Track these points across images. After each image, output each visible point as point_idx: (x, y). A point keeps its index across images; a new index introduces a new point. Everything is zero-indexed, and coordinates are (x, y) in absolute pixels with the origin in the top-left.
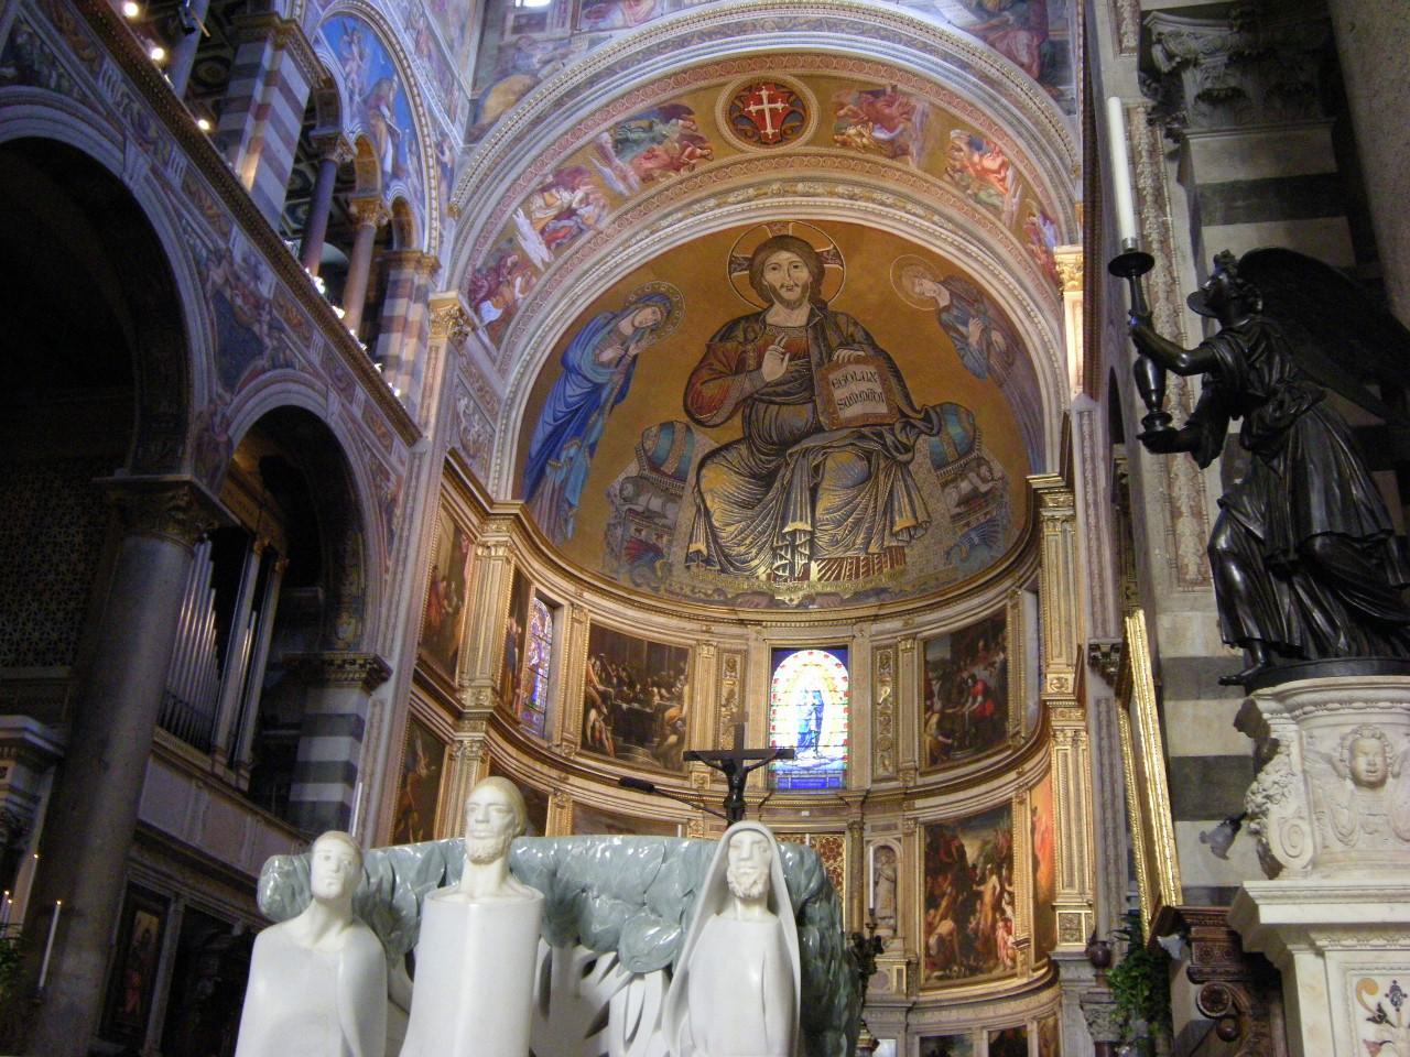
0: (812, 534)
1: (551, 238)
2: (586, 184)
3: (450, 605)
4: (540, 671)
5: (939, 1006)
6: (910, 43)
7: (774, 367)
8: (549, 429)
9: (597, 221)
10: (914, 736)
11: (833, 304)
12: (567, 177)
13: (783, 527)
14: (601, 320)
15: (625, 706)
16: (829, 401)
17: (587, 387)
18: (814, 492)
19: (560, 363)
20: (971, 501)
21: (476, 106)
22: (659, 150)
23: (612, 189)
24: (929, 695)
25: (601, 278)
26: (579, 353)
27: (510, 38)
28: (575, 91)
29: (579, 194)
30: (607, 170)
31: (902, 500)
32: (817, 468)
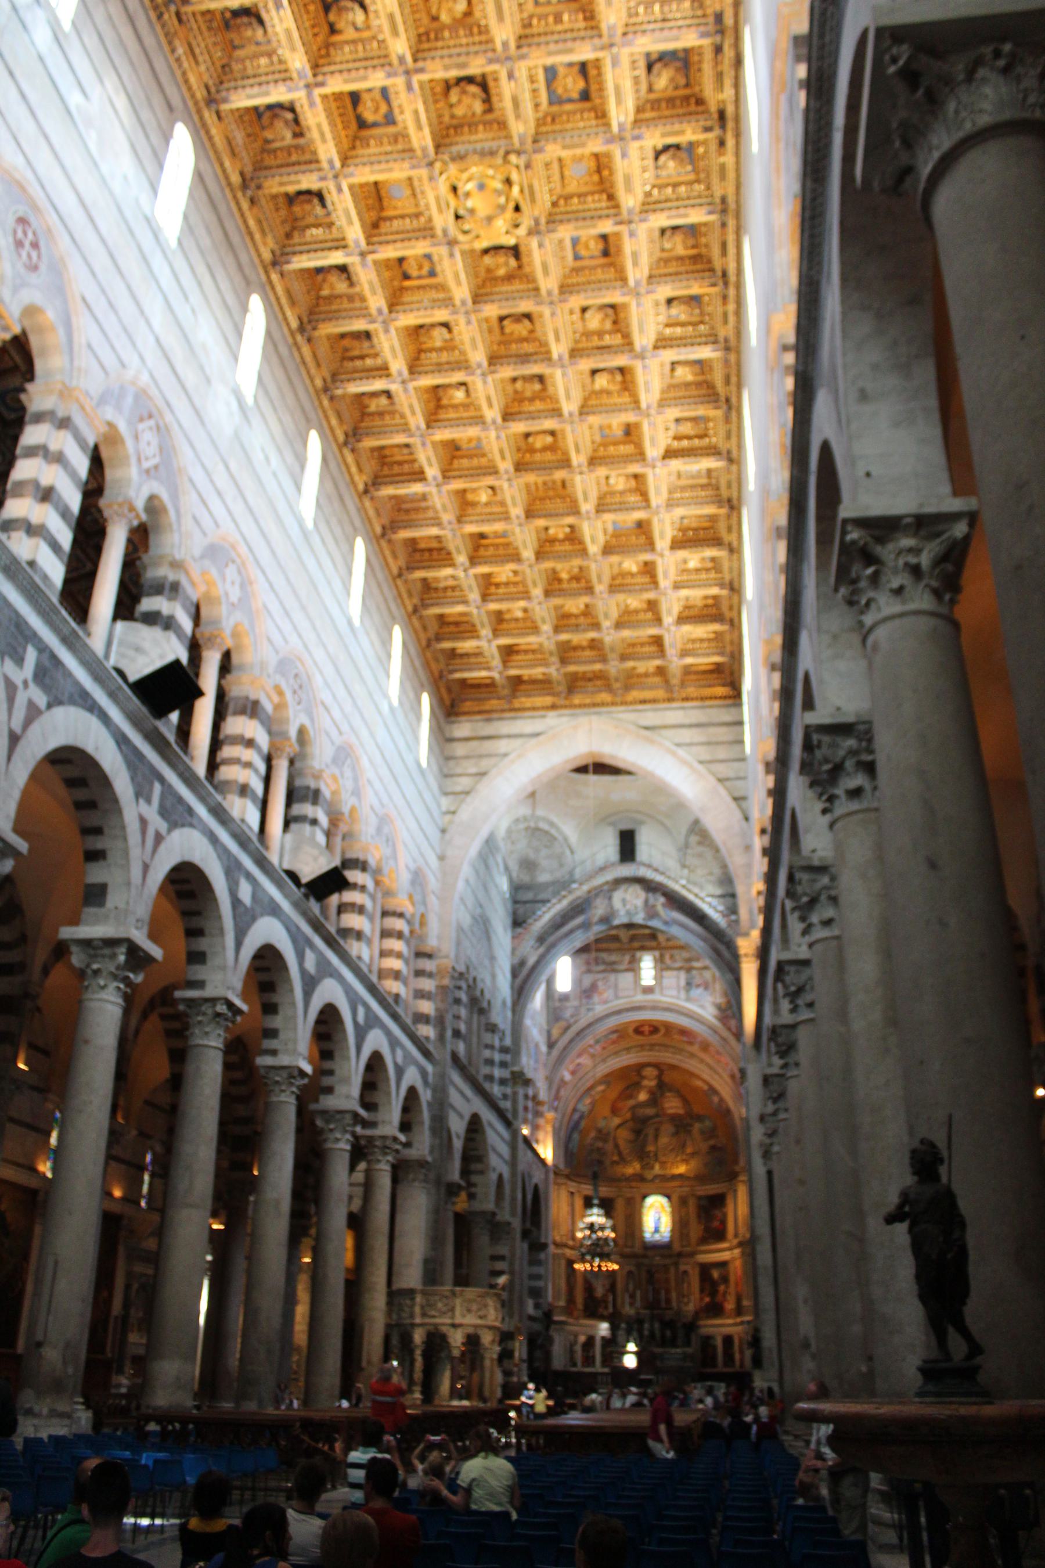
1: (573, 1073)
5: (705, 1326)
6: (698, 1020)
7: (643, 1096)
10: (695, 1231)
11: (666, 1079)
12: (579, 1055)
16: (663, 1109)
18: (656, 1137)
19: (575, 1110)
20: (713, 1148)
21: (549, 1034)
24: (699, 1217)
27: (557, 1004)
28: (583, 1030)
31: (689, 1143)
32: (657, 1130)
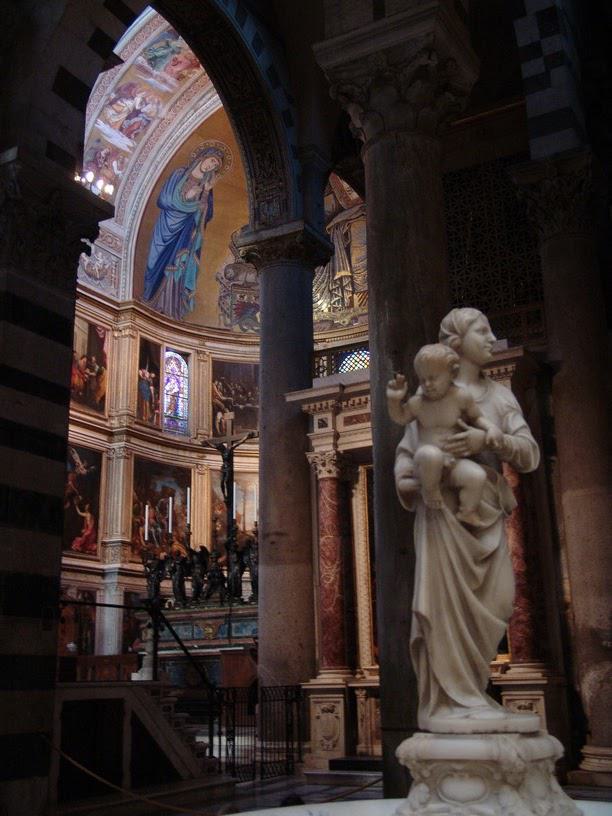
0: (351, 277)
1: (128, 132)
2: (141, 92)
3: (92, 370)
4: (181, 395)
8: (161, 249)
9: (157, 112)
13: (334, 275)
14: (177, 174)
15: (241, 407)
17: (182, 217)
18: (348, 250)
22: (180, 57)
23: (160, 90)
25: (170, 148)
26: (170, 197)
29: (138, 100)
30: (151, 80)
32: (346, 234)
